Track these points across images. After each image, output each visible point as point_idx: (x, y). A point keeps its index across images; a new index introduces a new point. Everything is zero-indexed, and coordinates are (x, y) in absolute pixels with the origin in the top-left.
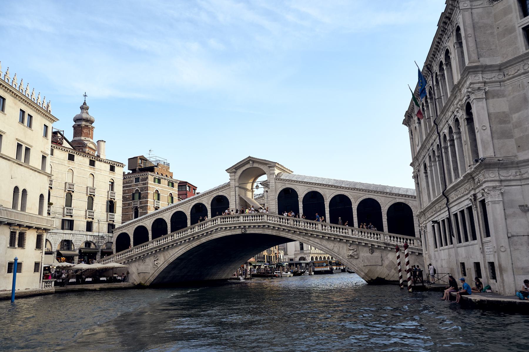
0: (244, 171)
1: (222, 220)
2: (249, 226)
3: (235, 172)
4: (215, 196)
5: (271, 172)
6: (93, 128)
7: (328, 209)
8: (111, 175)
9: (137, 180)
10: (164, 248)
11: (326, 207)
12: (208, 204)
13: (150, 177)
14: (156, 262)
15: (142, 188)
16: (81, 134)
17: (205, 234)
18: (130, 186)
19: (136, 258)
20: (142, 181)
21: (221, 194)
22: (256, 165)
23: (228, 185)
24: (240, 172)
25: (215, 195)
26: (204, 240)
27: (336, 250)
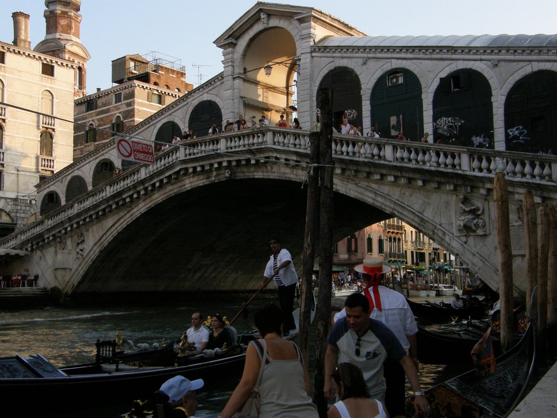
0: (252, 40)
1: (187, 152)
2: (239, 161)
3: (233, 45)
4: (196, 102)
5: (304, 32)
6: (80, 16)
7: (431, 113)
8: (47, 82)
9: (118, 99)
10: (91, 216)
11: (425, 107)
12: (184, 122)
13: (137, 91)
14: (80, 247)
15: (126, 111)
16: (56, 28)
17: (157, 184)
18: (108, 111)
19: (48, 238)
20: (125, 99)
21: (206, 97)
22: (274, 22)
23: (220, 77)
24: (243, 43)
25: (195, 101)
26: (158, 197)
27: (428, 214)
